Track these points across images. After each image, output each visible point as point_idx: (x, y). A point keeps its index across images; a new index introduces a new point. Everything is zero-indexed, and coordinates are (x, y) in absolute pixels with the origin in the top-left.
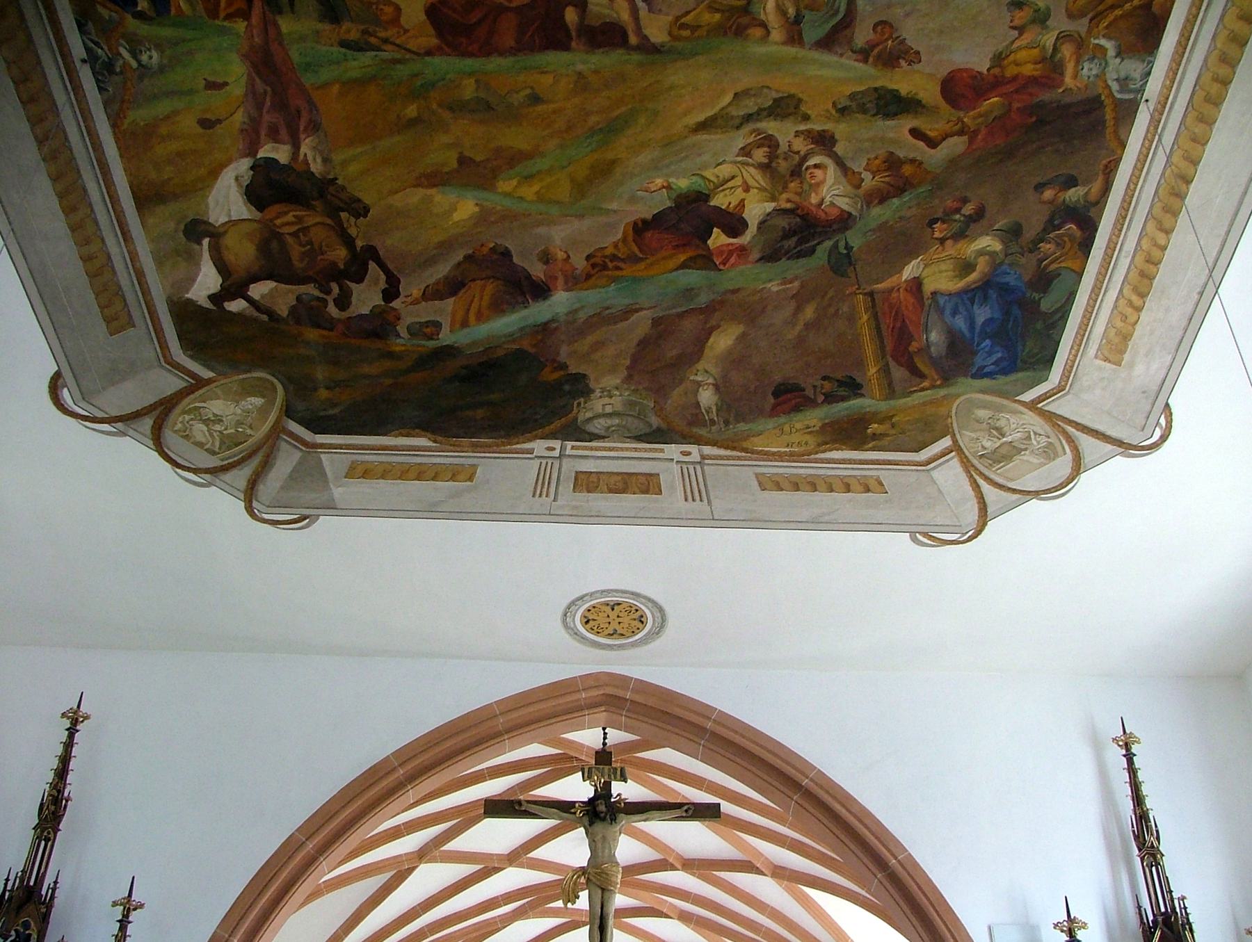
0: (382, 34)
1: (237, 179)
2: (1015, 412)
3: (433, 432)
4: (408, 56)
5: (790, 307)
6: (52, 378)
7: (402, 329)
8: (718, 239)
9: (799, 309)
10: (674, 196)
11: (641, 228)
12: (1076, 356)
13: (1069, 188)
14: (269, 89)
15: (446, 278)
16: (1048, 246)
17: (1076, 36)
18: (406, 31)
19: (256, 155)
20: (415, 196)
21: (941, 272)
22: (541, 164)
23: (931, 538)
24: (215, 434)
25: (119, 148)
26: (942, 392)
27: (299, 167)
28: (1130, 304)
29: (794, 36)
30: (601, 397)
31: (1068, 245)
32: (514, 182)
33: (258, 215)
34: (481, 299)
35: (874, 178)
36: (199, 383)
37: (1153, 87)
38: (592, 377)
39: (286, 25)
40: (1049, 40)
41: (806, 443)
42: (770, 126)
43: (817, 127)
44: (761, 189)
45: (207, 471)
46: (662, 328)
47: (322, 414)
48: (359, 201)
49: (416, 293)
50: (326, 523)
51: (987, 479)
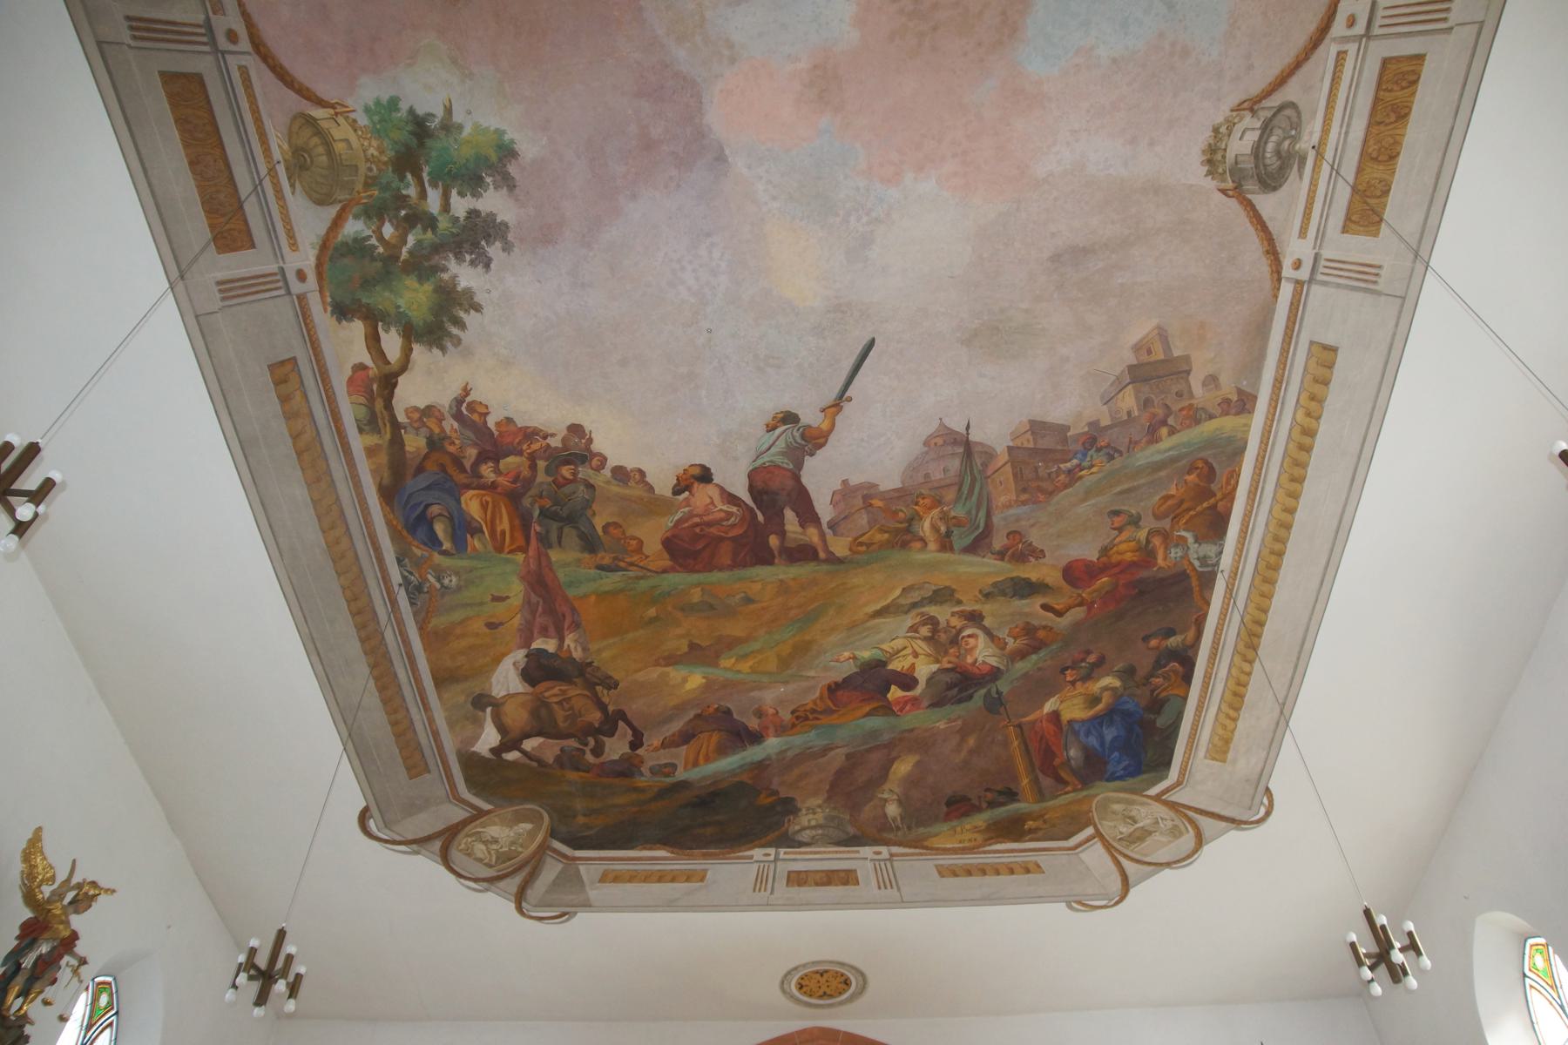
1: (514, 664)
2: (1142, 804)
3: (671, 846)
4: (649, 574)
6: (362, 812)
8: (895, 693)
9: (963, 739)
10: (859, 663)
11: (833, 689)
12: (1189, 759)
13: (1170, 637)
14: (541, 602)
16: (1158, 680)
18: (647, 557)
20: (654, 673)
21: (1074, 705)
22: (756, 646)
23: (1084, 905)
24: (492, 852)
26: (1085, 793)
28: (1228, 716)
29: (946, 544)
31: (1173, 678)
32: (733, 660)
33: (529, 689)
34: (708, 746)
36: (480, 814)
37: (1226, 561)
39: (555, 555)
40: (1142, 535)
42: (932, 610)
43: (969, 608)
44: (928, 655)
45: (484, 880)
47: (579, 835)
48: (611, 677)
49: (656, 742)
50: (583, 918)
51: (1125, 856)
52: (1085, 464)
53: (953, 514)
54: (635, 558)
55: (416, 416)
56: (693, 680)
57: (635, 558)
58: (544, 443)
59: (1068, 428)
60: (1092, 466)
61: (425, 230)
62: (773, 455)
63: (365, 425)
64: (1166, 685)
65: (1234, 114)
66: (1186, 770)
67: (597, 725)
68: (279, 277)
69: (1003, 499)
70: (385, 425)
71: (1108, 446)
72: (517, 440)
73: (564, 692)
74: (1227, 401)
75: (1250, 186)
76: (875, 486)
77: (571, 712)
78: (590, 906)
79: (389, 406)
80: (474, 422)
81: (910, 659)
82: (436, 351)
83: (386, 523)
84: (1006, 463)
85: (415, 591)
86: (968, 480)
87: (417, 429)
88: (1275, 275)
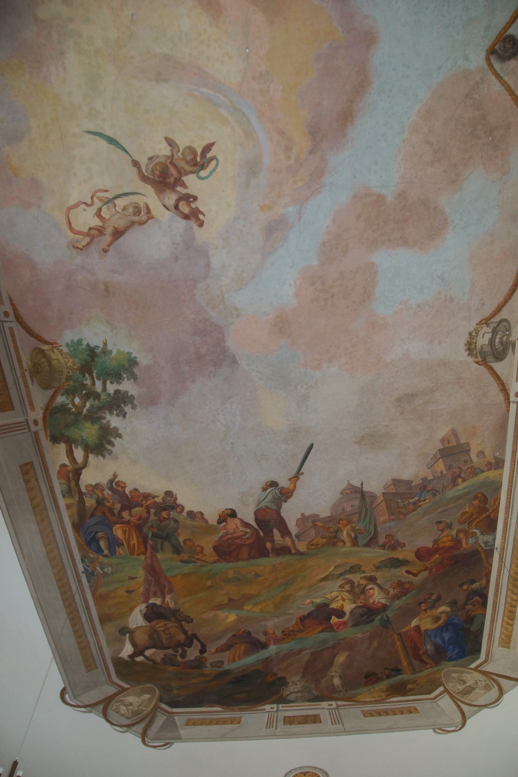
0: (197, 557)
1: (140, 611)
4: (207, 564)
7: (208, 664)
8: (334, 620)
11: (302, 619)
12: (490, 647)
13: (473, 584)
14: (153, 579)
16: (469, 607)
17: (464, 530)
18: (206, 555)
20: (211, 614)
21: (427, 622)
24: (130, 711)
25: (95, 602)
26: (436, 668)
28: (508, 624)
29: (355, 543)
30: (292, 685)
32: (251, 606)
33: (148, 624)
35: (394, 590)
36: (124, 690)
37: (498, 543)
39: (160, 556)
40: (454, 533)
41: (381, 696)
42: (351, 577)
43: (369, 575)
44: (350, 600)
46: (315, 656)
48: (189, 617)
49: (213, 650)
50: (177, 746)
51: (462, 702)
52: (422, 499)
53: (357, 527)
54: (199, 556)
55: (91, 489)
56: (232, 617)
57: (199, 556)
59: (412, 482)
60: (425, 500)
61: (94, 400)
62: (268, 502)
63: (66, 493)
64: (474, 609)
65: (478, 326)
66: (489, 654)
67: (182, 642)
68: (25, 424)
69: (382, 519)
70: (76, 493)
71: (433, 489)
72: (140, 500)
73: (165, 625)
74: (490, 463)
75: (490, 359)
77: (169, 635)
78: (181, 739)
79: (77, 485)
80: (119, 491)
81: (341, 602)
82: (100, 457)
83: (76, 542)
84: (382, 501)
85: (90, 575)
86: (364, 510)
87: (91, 495)
88: (507, 401)
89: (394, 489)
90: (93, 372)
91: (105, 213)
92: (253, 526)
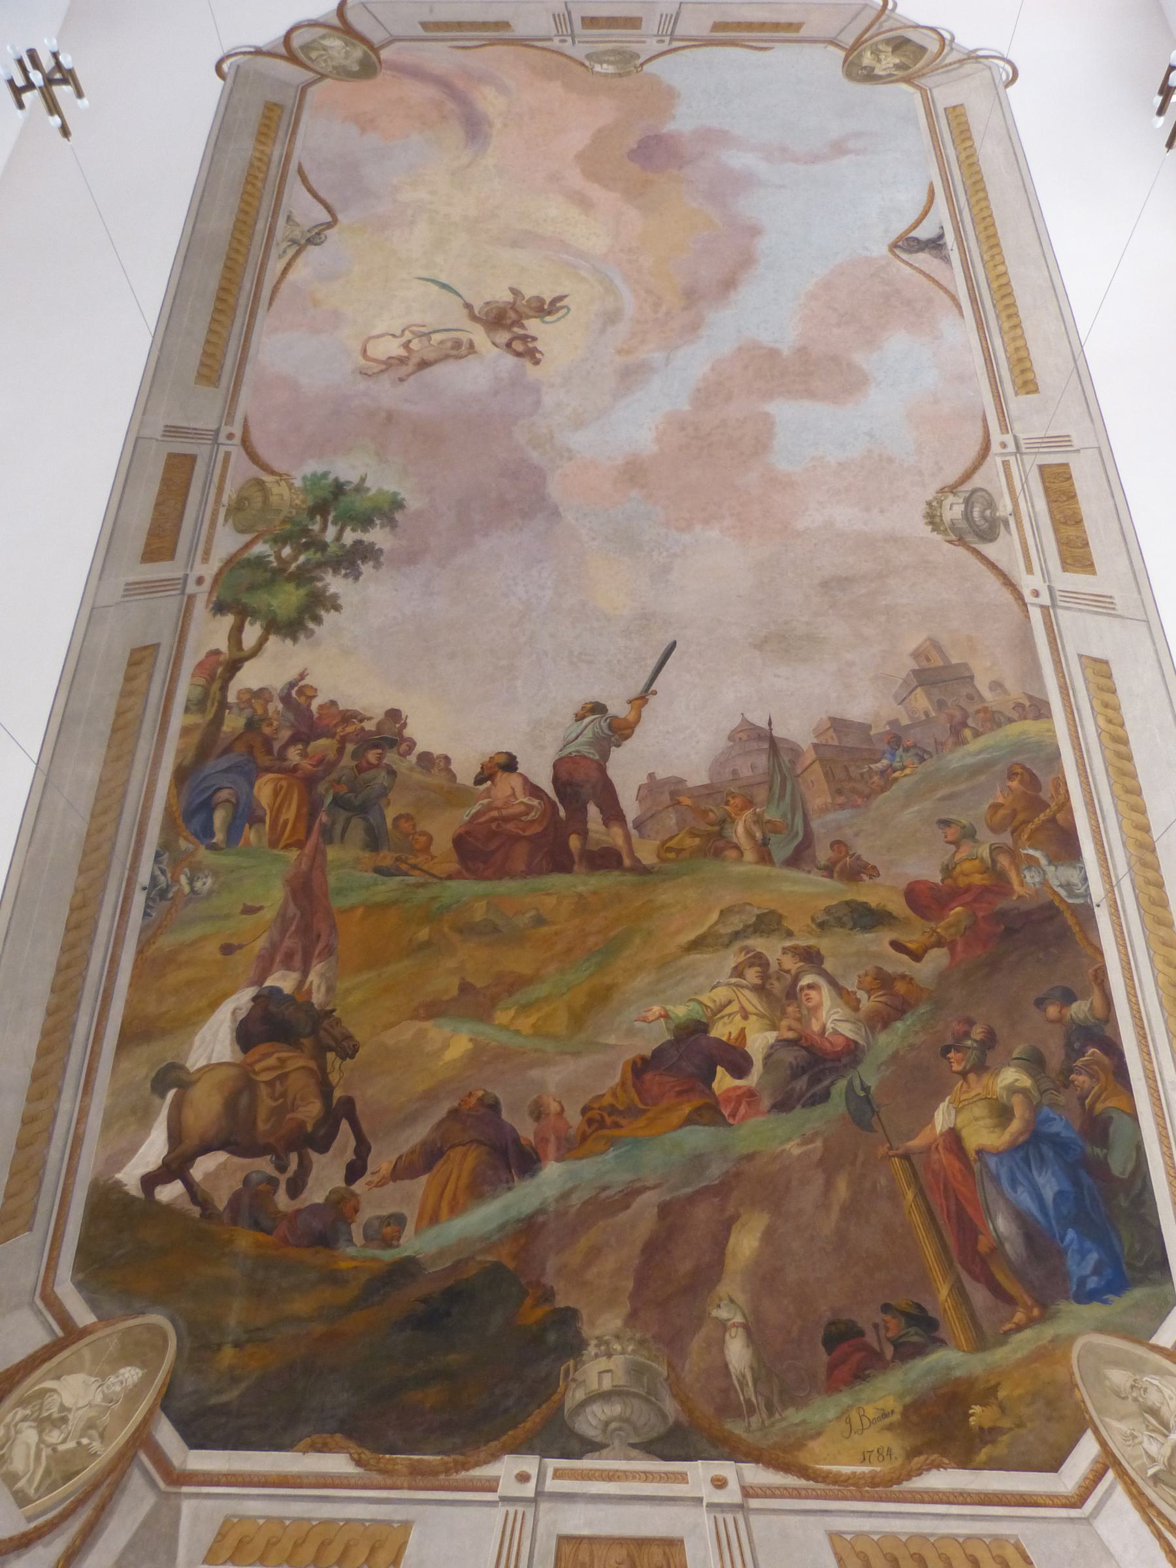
0: (412, 861)
3: (361, 1443)
5: (819, 1179)
8: (723, 1081)
9: (829, 1185)
10: (672, 1026)
11: (641, 1068)
13: (1071, 1004)
14: (298, 913)
15: (424, 1143)
18: (433, 858)
19: (262, 984)
20: (408, 1031)
22: (541, 990)
27: (300, 999)
29: (765, 857)
31: (1102, 1077)
34: (459, 1178)
35: (869, 997)
38: (584, 1313)
39: (333, 853)
40: (984, 852)
42: (758, 944)
43: (802, 942)
44: (761, 1016)
47: (213, 1401)
53: (767, 817)
54: (418, 860)
57: (418, 860)
58: (359, 726)
59: (870, 727)
61: (315, 552)
62: (582, 744)
64: (1096, 1088)
70: (213, 704)
72: (334, 722)
73: (282, 1061)
75: (970, 538)
76: (681, 781)
79: (224, 688)
80: (299, 704)
82: (289, 642)
83: (166, 809)
84: (814, 762)
85: (157, 893)
86: (778, 779)
89: (835, 738)
90: (329, 514)
91: (415, 345)
92: (546, 794)
